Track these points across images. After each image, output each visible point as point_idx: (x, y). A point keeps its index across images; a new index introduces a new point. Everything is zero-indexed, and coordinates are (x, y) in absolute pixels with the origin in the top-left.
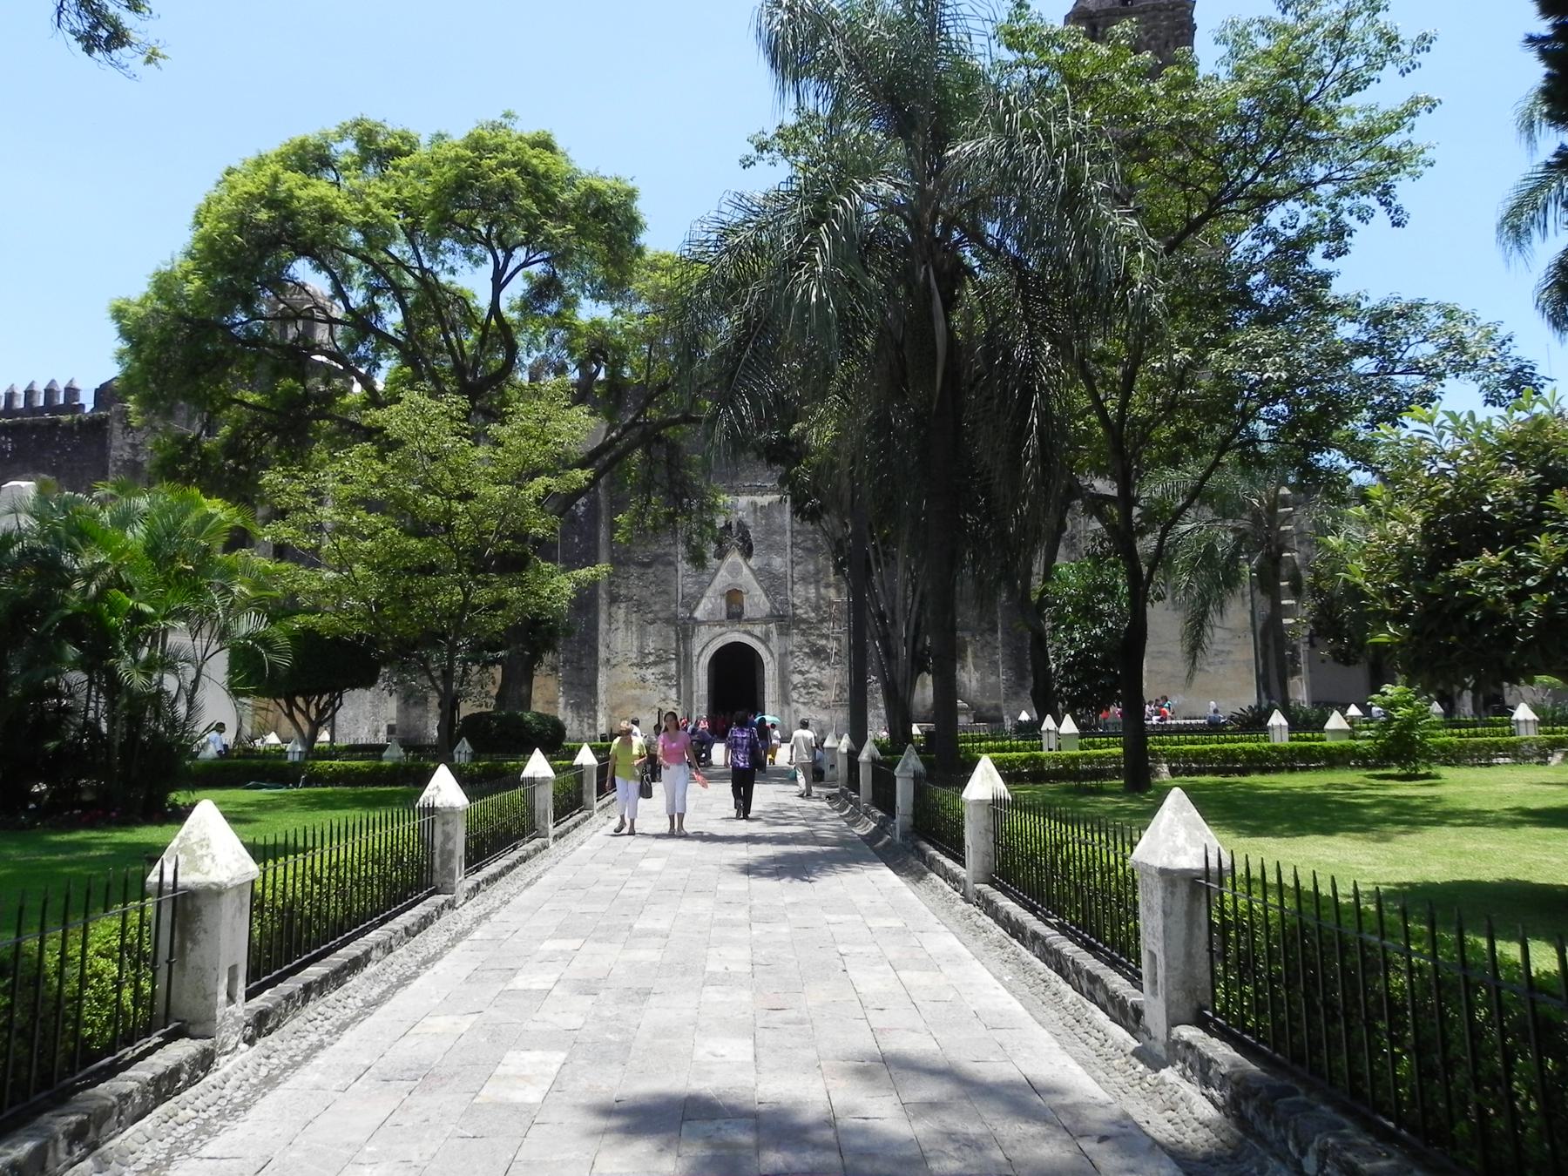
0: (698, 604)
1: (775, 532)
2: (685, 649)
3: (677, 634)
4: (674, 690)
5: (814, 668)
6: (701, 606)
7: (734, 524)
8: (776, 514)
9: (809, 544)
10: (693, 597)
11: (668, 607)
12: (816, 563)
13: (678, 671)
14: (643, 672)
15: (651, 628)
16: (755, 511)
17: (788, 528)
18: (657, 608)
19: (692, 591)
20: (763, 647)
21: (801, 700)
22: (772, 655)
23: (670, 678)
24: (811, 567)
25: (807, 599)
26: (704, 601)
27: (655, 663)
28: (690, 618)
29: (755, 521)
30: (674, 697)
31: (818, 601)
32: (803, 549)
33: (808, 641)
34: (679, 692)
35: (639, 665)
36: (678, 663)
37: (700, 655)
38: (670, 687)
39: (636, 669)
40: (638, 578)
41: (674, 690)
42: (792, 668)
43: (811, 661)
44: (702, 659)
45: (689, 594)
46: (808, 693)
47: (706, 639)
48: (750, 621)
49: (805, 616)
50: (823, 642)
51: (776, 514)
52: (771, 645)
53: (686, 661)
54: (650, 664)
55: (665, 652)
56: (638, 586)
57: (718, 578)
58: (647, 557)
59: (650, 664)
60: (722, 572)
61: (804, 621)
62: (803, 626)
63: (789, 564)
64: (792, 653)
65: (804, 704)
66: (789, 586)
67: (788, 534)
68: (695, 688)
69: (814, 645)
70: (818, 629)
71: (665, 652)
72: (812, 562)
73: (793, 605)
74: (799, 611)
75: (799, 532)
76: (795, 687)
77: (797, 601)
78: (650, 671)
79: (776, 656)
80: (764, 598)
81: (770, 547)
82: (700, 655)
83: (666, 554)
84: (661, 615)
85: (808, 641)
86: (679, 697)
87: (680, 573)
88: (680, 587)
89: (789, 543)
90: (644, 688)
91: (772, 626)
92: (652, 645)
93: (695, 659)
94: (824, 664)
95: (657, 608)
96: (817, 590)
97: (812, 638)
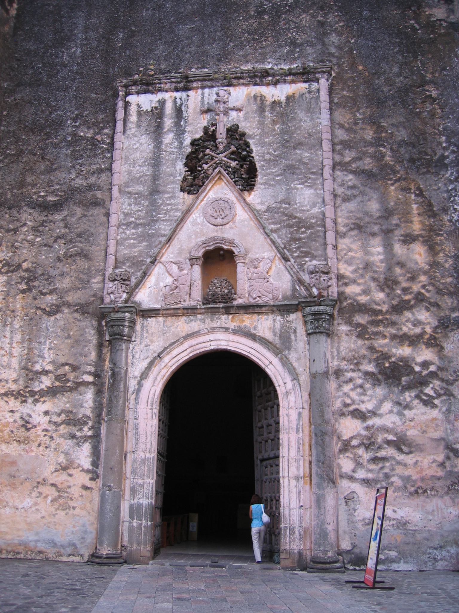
0: (145, 275)
1: (299, 145)
2: (113, 362)
3: (100, 333)
4: (87, 447)
5: (387, 406)
6: (151, 281)
7: (222, 137)
8: (301, 115)
9: (368, 163)
10: (136, 263)
11: (85, 284)
12: (383, 199)
13: (98, 409)
14: (26, 409)
15: (49, 322)
16: (262, 109)
17: (326, 136)
18: (65, 283)
19: (135, 252)
20: (276, 361)
21: (361, 474)
22: (295, 377)
23: (78, 423)
24: (374, 206)
25: (367, 266)
26: (158, 269)
27: (52, 392)
28: (126, 301)
29: (261, 124)
30: (86, 462)
31: (390, 269)
32: (354, 172)
33: (372, 349)
34: (96, 453)
35: (19, 395)
36: (99, 392)
37: (144, 375)
38: (79, 441)
39: (13, 403)
40: (35, 229)
41: (87, 448)
42: (338, 404)
43: (380, 391)
44: (147, 384)
45: (128, 259)
46: (375, 460)
47: (157, 346)
48: (247, 308)
49: (363, 299)
50: (405, 351)
51: (301, 115)
52: (293, 356)
53: (113, 387)
54: (43, 393)
55: (75, 368)
56: (32, 243)
57: (188, 226)
58: (54, 193)
59: (43, 393)
60: (196, 216)
61: (362, 309)
62: (361, 319)
63: (328, 198)
64: (338, 373)
65: (366, 482)
66: (330, 236)
67: (326, 146)
68: (130, 445)
69: (386, 356)
70: (393, 324)
71: (75, 368)
72: (375, 196)
73: (340, 277)
74: (352, 290)
75: (347, 145)
76: (346, 447)
77: (346, 270)
78: (41, 407)
79: (304, 378)
80: (278, 264)
81: (291, 170)
82: (144, 375)
83: (90, 187)
84: (72, 297)
85: (372, 349)
86: (95, 464)
87: (114, 219)
88: (112, 244)
89: (328, 162)
90: (26, 441)
91: (295, 318)
92: (48, 355)
93: (133, 384)
94: (408, 396)
95: (65, 283)
96: (388, 246)
97: (381, 343)
